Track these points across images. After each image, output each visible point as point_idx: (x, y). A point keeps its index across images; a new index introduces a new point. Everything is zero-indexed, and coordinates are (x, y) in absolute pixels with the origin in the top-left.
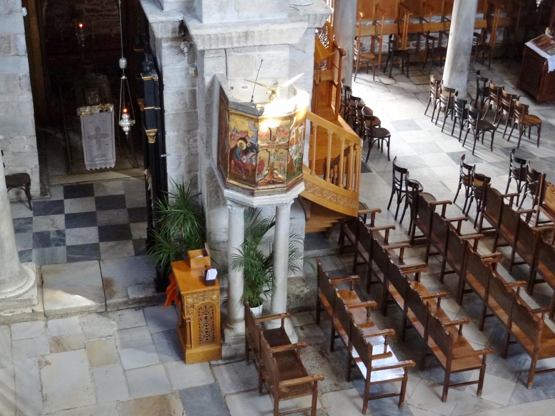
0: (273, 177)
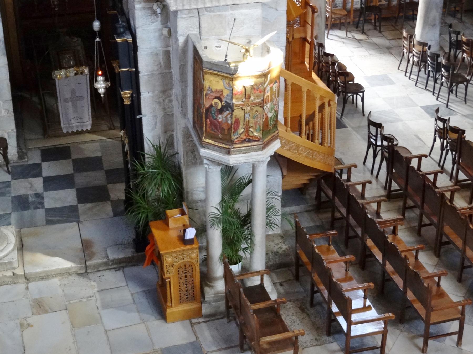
0: (249, 135)
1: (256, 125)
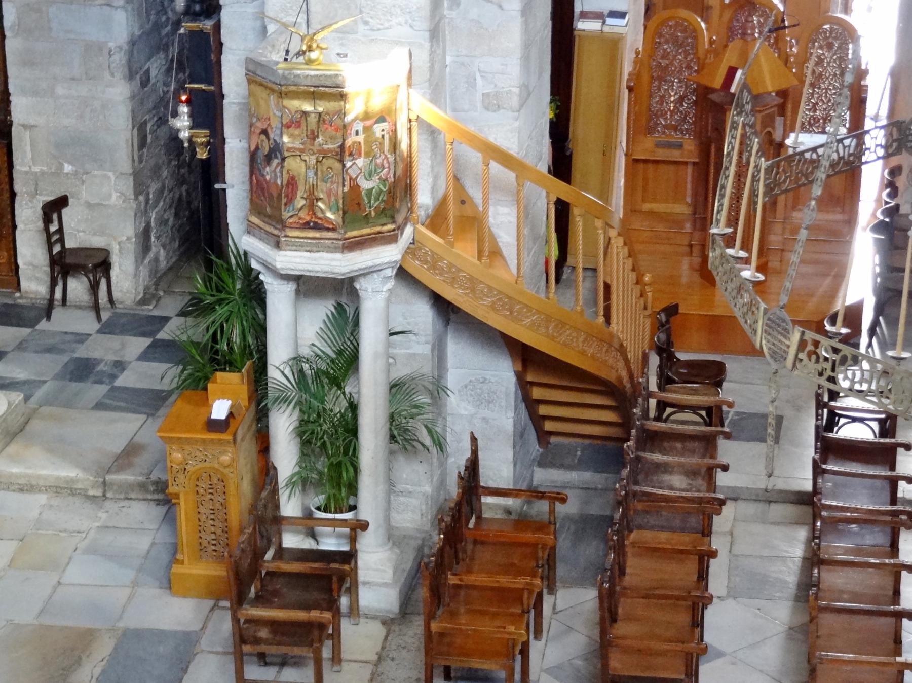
0: (314, 214)
1: (329, 196)
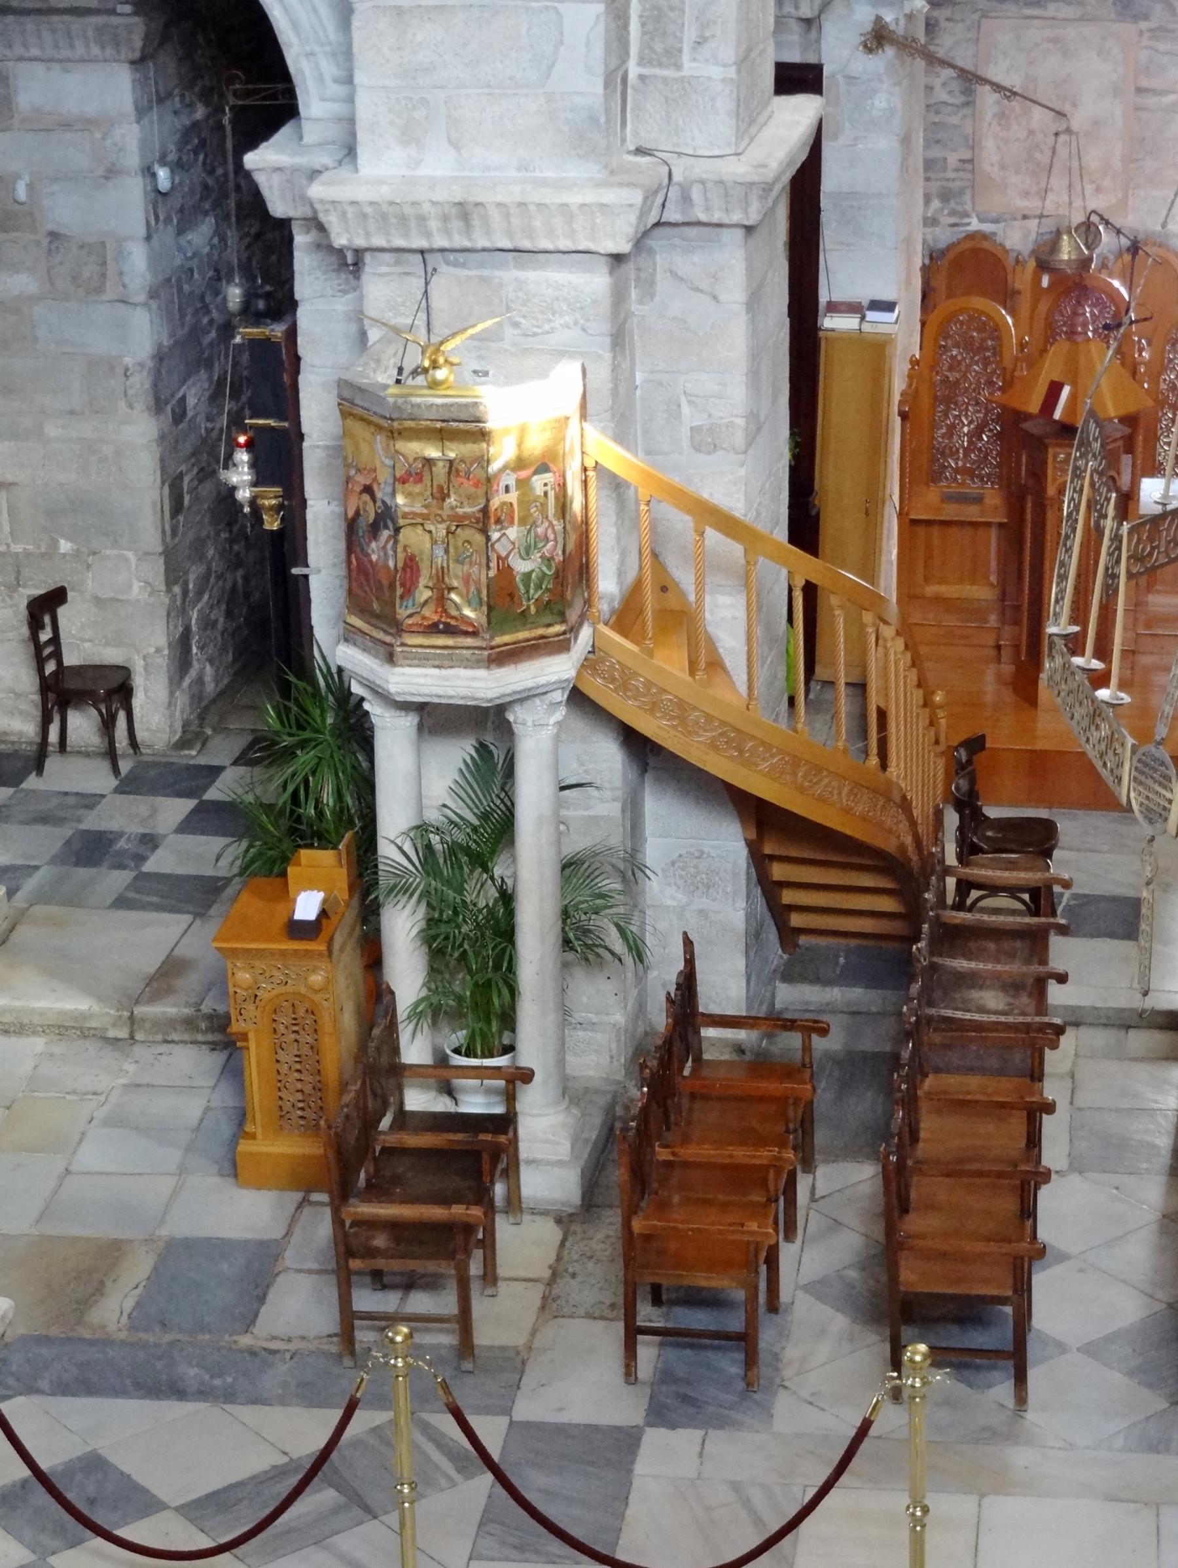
0: (445, 611)
